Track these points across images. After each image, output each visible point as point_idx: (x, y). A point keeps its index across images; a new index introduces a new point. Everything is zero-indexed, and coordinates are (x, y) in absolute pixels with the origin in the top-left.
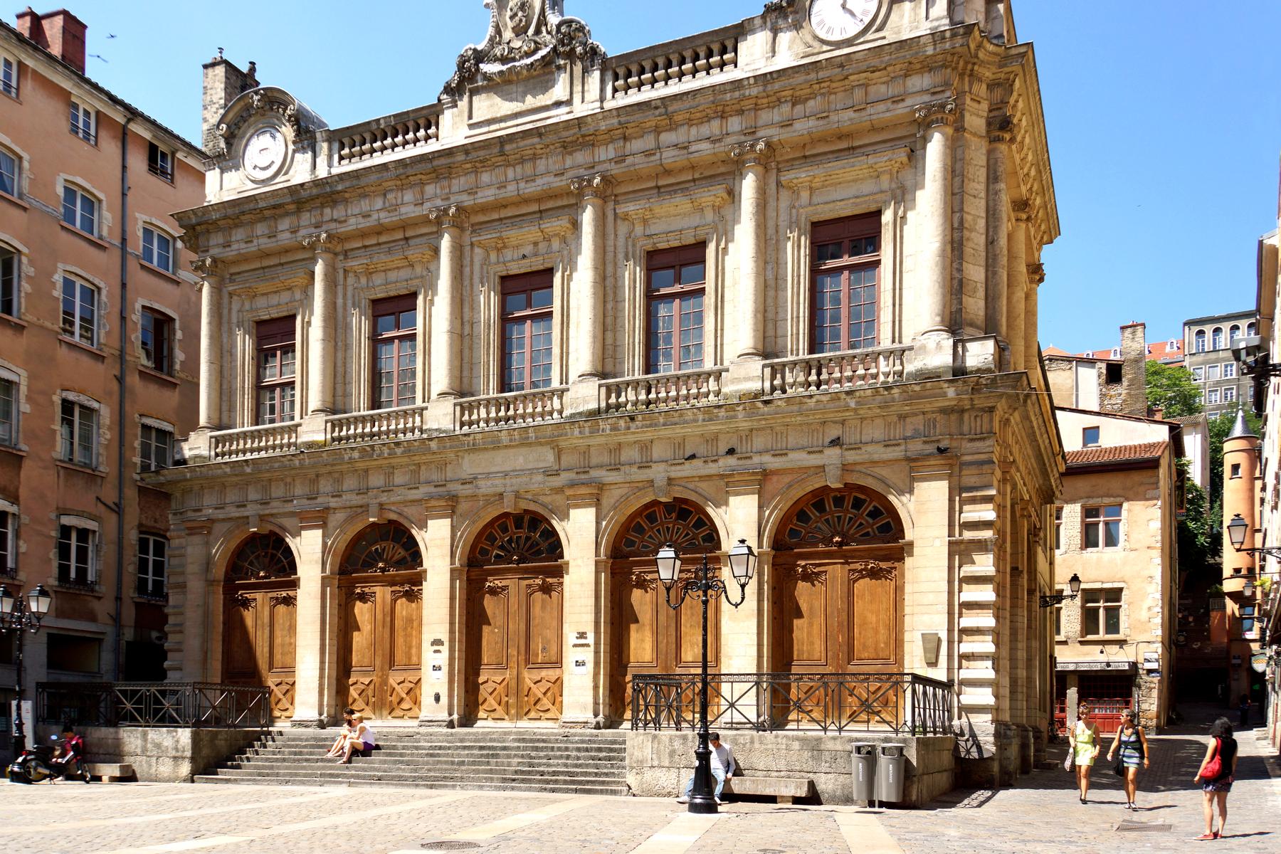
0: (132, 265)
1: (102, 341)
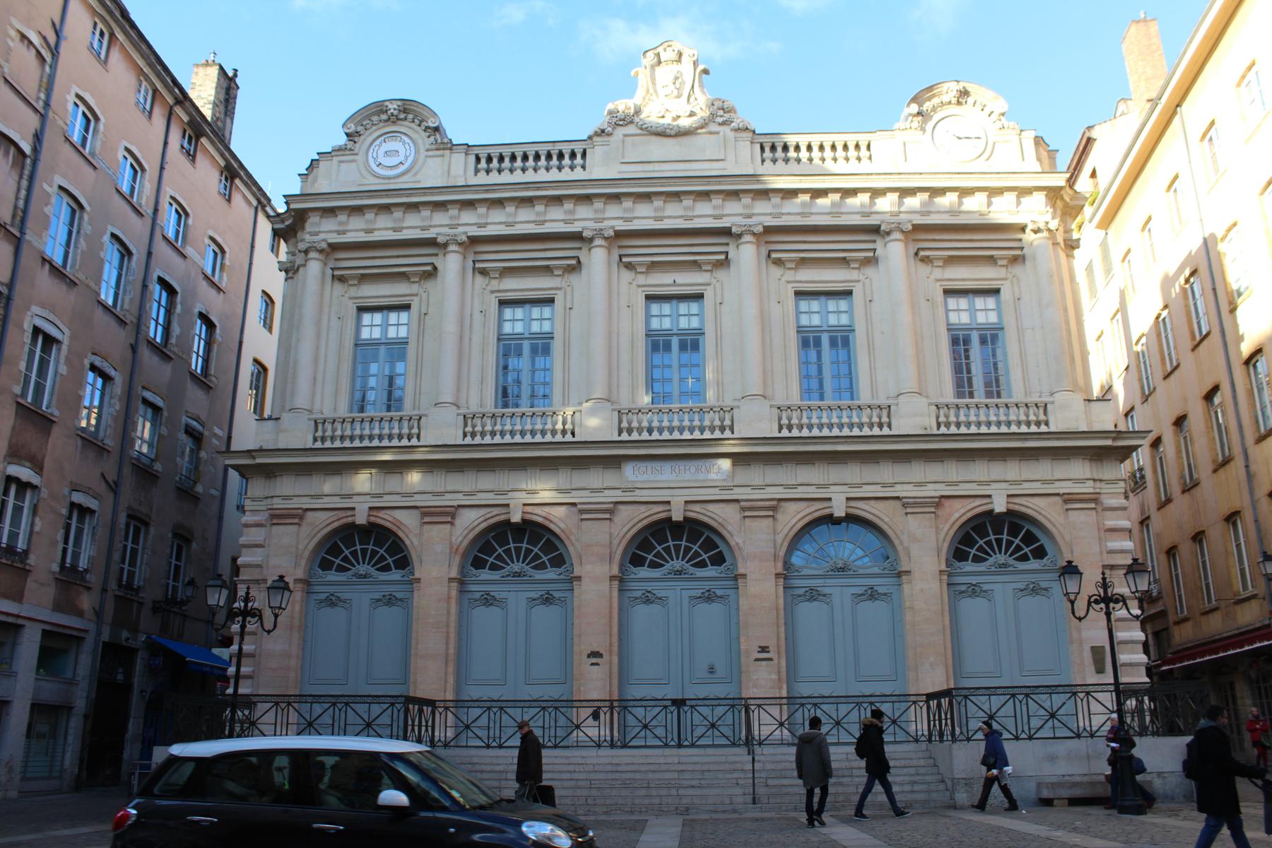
0: (158, 236)
1: (126, 306)
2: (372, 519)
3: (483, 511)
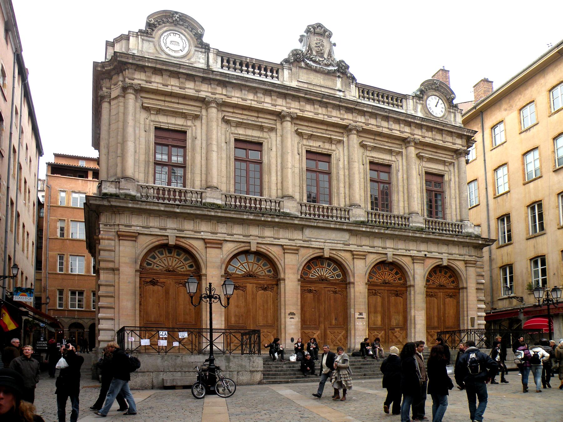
2: (178, 242)
3: (236, 244)
